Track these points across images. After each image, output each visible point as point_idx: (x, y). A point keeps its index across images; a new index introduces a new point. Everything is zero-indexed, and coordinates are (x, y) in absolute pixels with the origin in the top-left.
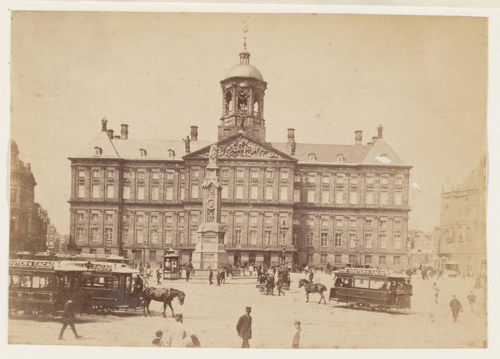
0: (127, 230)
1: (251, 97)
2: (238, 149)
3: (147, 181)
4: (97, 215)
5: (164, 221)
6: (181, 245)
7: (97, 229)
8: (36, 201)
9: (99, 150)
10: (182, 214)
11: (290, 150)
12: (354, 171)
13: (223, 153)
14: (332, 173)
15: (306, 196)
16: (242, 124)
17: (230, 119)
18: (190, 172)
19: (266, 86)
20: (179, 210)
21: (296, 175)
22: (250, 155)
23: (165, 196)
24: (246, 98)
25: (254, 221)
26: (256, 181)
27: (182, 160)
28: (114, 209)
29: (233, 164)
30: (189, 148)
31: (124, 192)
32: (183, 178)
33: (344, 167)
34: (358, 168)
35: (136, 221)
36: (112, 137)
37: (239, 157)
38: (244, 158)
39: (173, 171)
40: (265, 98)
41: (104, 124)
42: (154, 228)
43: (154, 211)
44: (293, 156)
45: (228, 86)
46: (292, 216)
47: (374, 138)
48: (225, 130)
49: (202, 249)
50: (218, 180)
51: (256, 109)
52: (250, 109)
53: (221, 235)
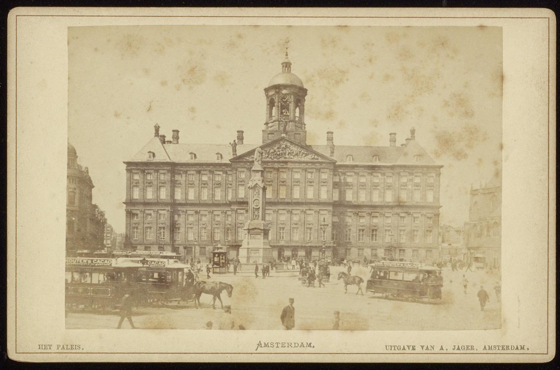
0: (179, 228)
1: (292, 103)
2: (281, 152)
3: (196, 183)
7: (150, 228)
8: (93, 203)
9: (152, 154)
11: (329, 152)
12: (389, 170)
13: (267, 155)
15: (345, 194)
16: (285, 128)
17: (273, 124)
18: (236, 173)
19: (306, 92)
20: (226, 209)
22: (292, 157)
23: (213, 195)
24: (288, 105)
25: (283, 218)
27: (229, 162)
28: (166, 208)
30: (236, 151)
32: (230, 179)
34: (392, 167)
35: (186, 219)
36: (164, 142)
37: (282, 159)
38: (287, 160)
39: (221, 173)
41: (157, 129)
42: (203, 226)
44: (332, 158)
45: (271, 93)
46: (331, 213)
47: (407, 140)
48: (270, 134)
49: (248, 245)
50: (263, 181)
51: (297, 114)
52: (292, 115)
53: (266, 233)
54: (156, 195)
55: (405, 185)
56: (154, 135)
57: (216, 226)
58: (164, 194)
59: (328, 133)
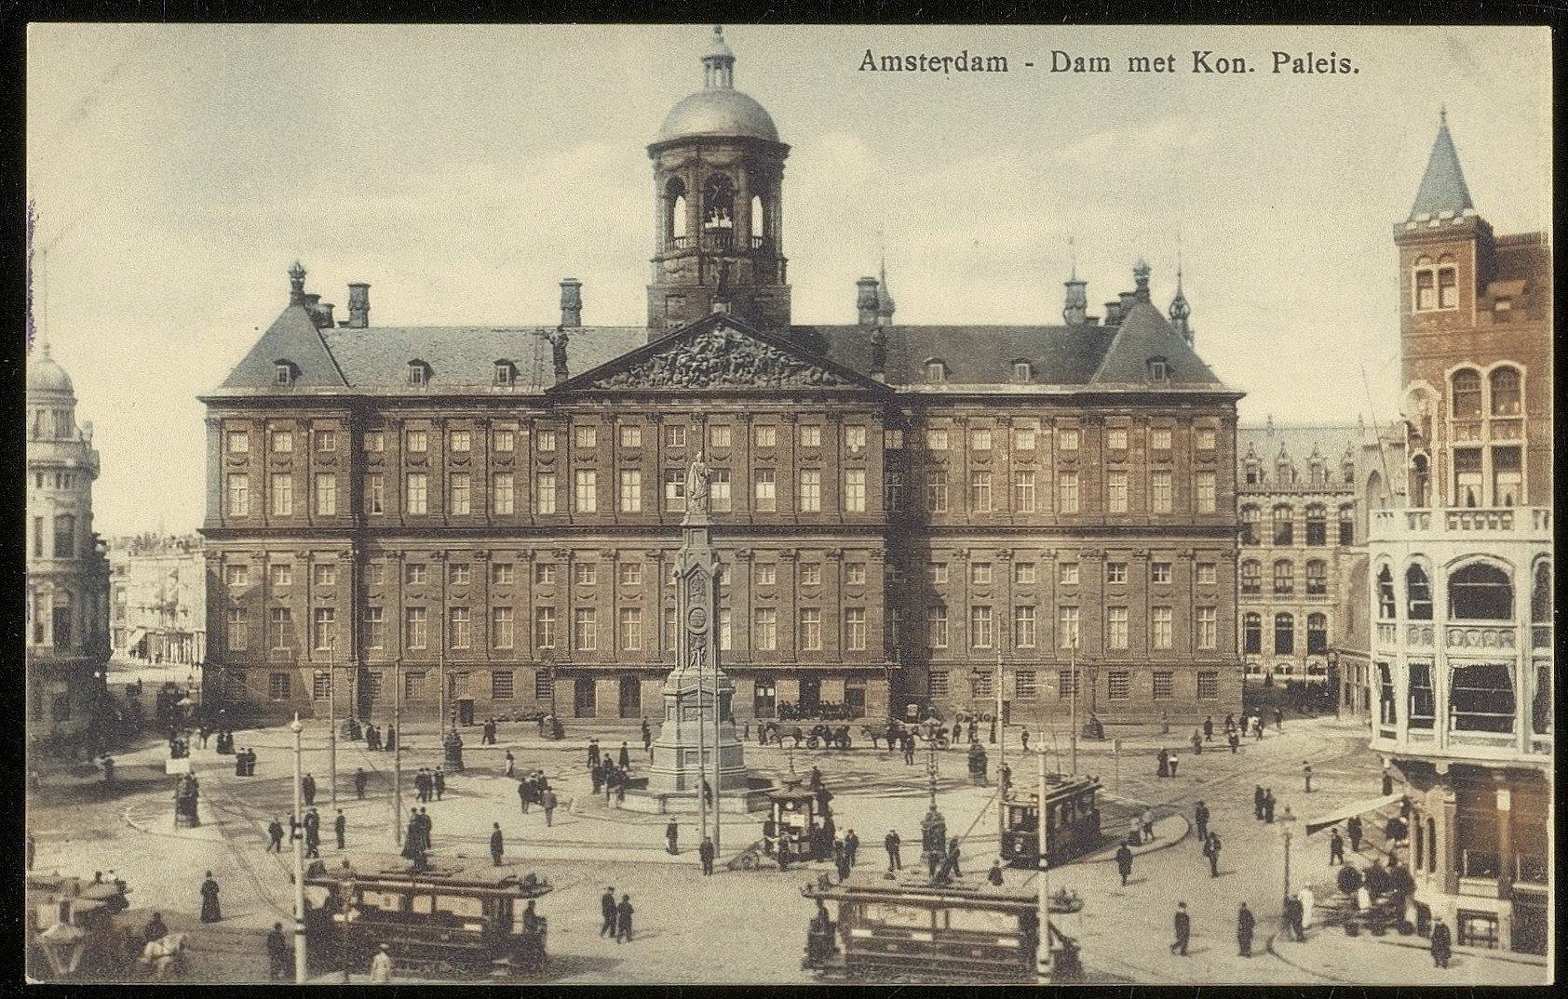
0: (379, 610)
18: (567, 433)
20: (533, 546)
23: (489, 503)
29: (698, 407)
39: (515, 426)
40: (789, 190)
44: (880, 378)
45: (670, 160)
46: (880, 561)
47: (1122, 295)
51: (757, 228)
54: (303, 503)
55: (1119, 456)
56: (287, 300)
57: (502, 603)
58: (329, 499)
59: (859, 284)
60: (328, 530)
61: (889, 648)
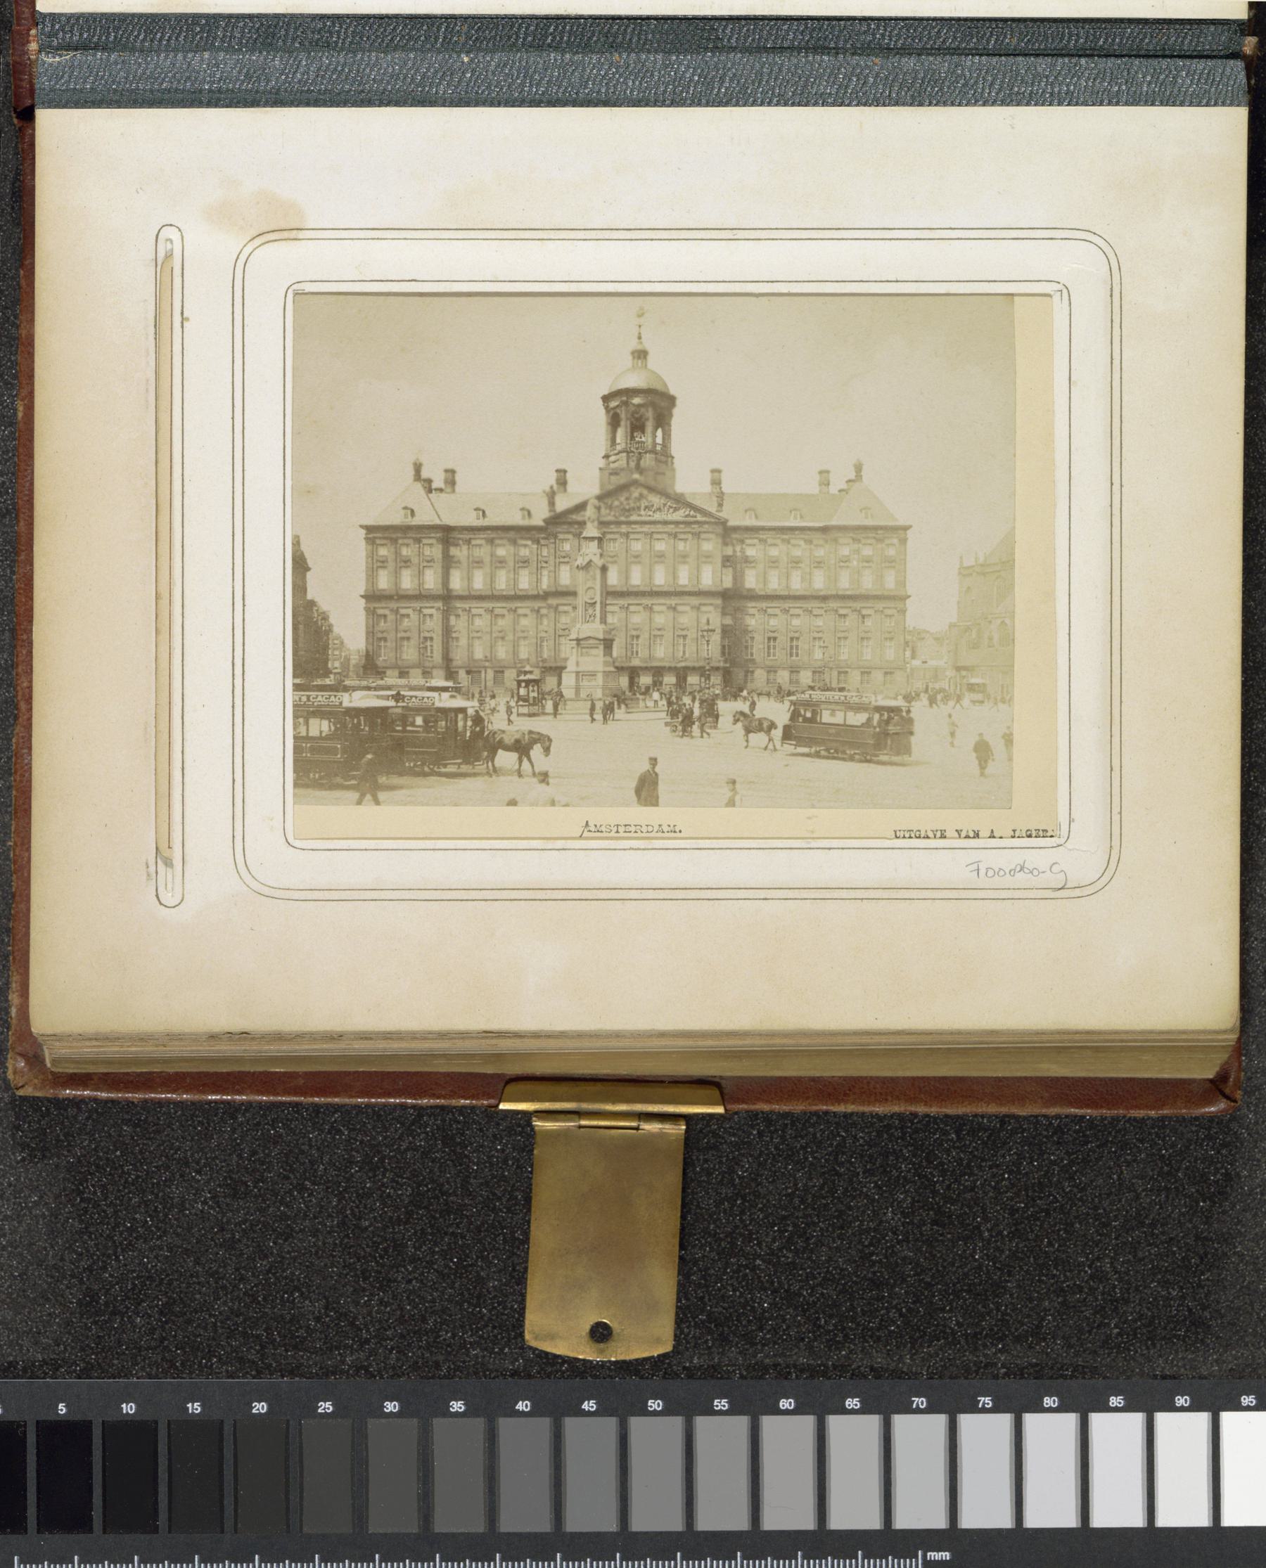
0: (457, 639)
3: (487, 559)
4: (408, 616)
5: (515, 622)
6: (544, 661)
7: (408, 639)
10: (544, 611)
11: (716, 504)
14: (783, 540)
21: (725, 544)
23: (515, 581)
26: (661, 556)
27: (541, 523)
29: (624, 529)
31: (452, 578)
32: (545, 553)
33: (802, 529)
34: (825, 530)
37: (634, 518)
38: (643, 519)
39: (529, 543)
43: (499, 607)
45: (613, 404)
48: (611, 474)
51: (659, 440)
52: (650, 440)
53: (608, 644)
55: (846, 560)
60: (434, 598)
61: (723, 653)
